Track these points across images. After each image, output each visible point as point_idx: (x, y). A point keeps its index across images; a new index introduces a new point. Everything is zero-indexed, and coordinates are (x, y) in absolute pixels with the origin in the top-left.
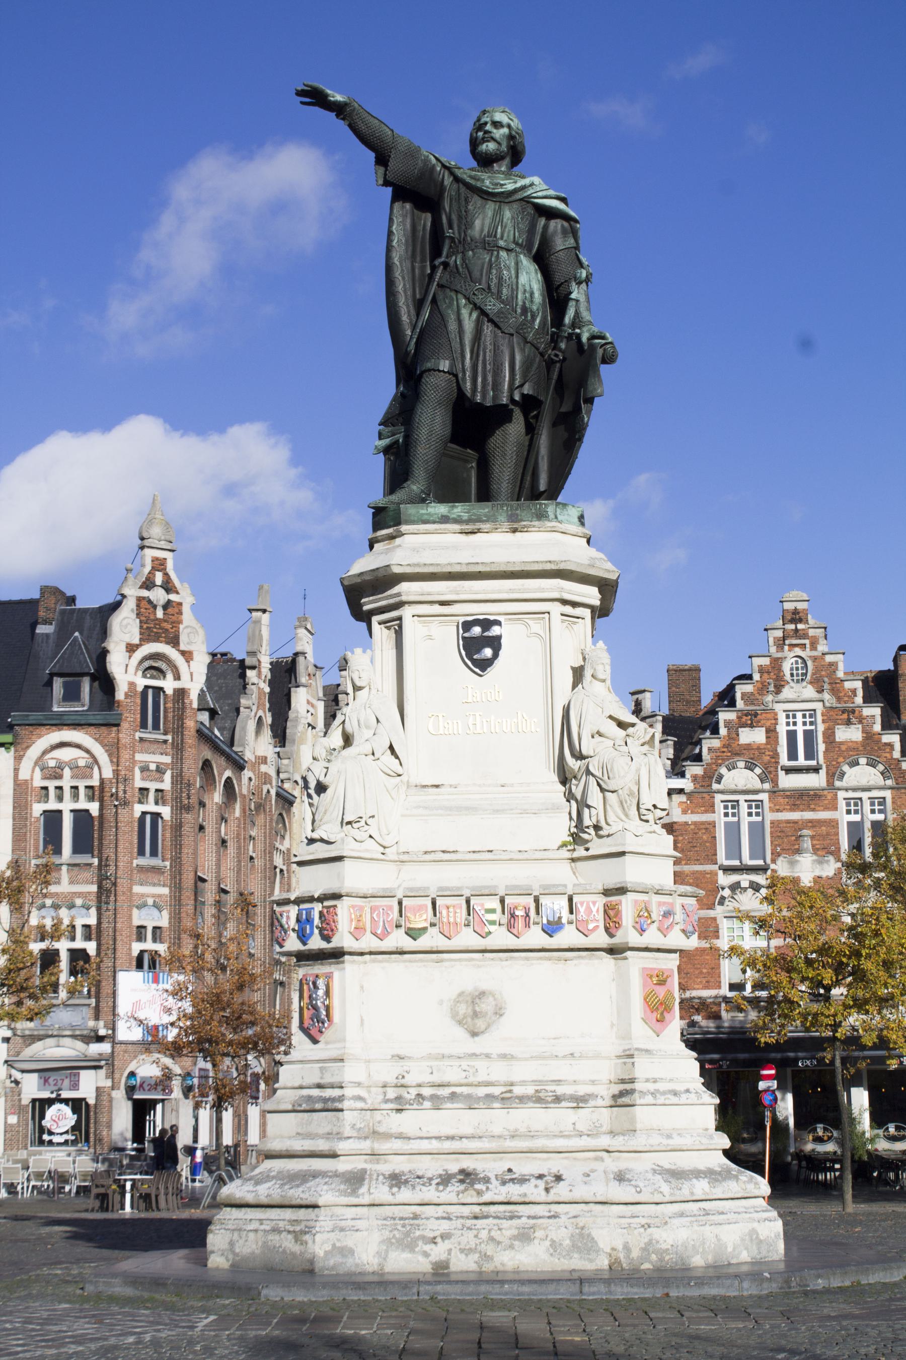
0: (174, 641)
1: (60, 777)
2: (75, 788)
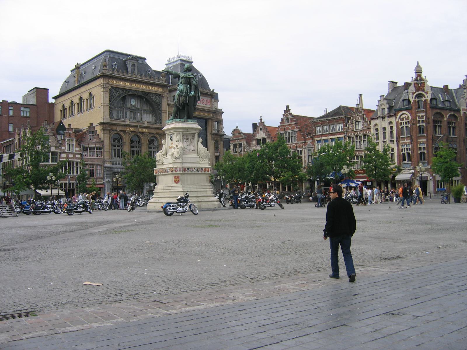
0: (423, 90)
1: (403, 120)
2: (406, 122)
